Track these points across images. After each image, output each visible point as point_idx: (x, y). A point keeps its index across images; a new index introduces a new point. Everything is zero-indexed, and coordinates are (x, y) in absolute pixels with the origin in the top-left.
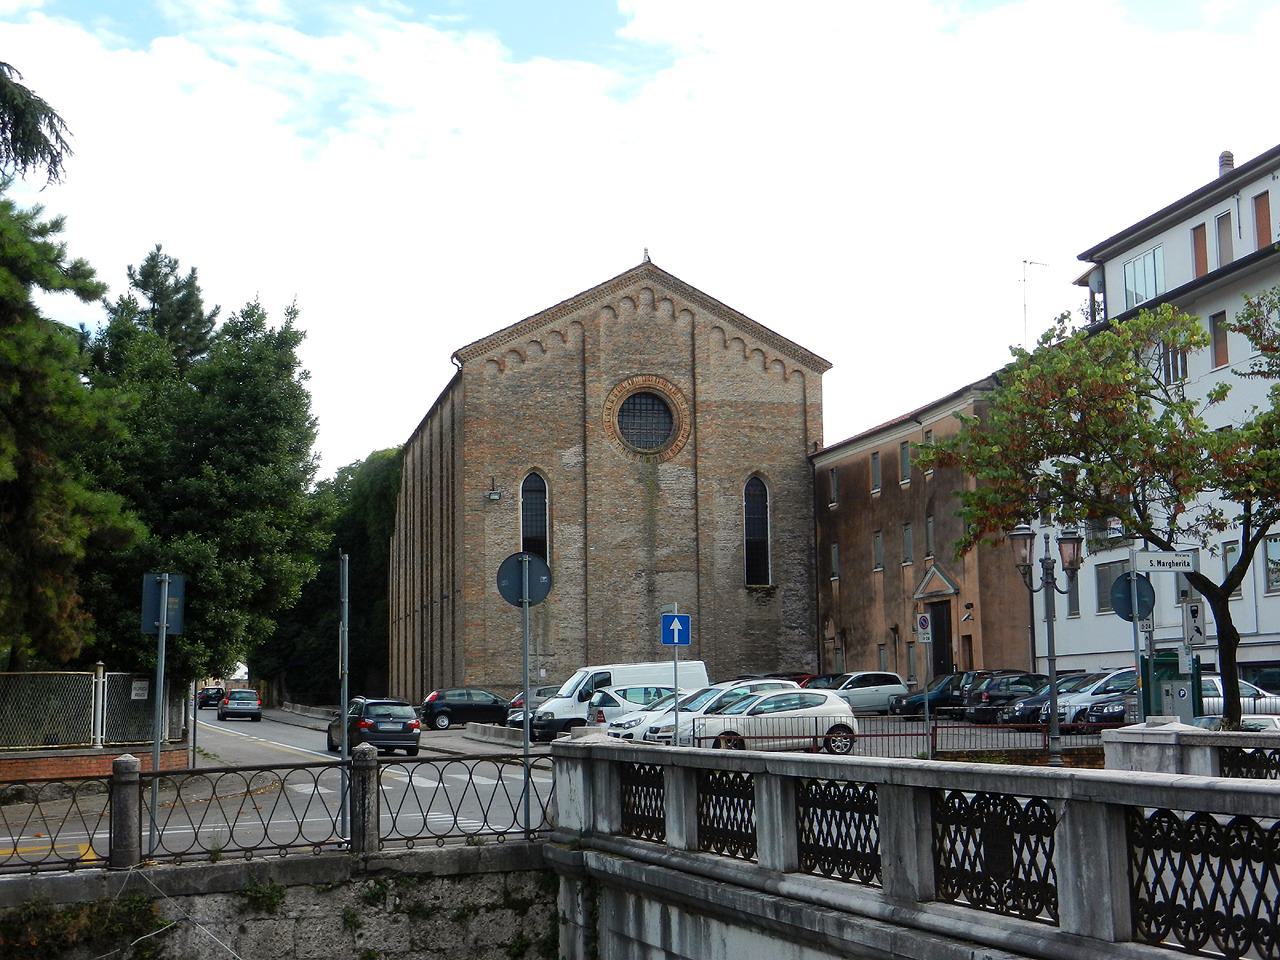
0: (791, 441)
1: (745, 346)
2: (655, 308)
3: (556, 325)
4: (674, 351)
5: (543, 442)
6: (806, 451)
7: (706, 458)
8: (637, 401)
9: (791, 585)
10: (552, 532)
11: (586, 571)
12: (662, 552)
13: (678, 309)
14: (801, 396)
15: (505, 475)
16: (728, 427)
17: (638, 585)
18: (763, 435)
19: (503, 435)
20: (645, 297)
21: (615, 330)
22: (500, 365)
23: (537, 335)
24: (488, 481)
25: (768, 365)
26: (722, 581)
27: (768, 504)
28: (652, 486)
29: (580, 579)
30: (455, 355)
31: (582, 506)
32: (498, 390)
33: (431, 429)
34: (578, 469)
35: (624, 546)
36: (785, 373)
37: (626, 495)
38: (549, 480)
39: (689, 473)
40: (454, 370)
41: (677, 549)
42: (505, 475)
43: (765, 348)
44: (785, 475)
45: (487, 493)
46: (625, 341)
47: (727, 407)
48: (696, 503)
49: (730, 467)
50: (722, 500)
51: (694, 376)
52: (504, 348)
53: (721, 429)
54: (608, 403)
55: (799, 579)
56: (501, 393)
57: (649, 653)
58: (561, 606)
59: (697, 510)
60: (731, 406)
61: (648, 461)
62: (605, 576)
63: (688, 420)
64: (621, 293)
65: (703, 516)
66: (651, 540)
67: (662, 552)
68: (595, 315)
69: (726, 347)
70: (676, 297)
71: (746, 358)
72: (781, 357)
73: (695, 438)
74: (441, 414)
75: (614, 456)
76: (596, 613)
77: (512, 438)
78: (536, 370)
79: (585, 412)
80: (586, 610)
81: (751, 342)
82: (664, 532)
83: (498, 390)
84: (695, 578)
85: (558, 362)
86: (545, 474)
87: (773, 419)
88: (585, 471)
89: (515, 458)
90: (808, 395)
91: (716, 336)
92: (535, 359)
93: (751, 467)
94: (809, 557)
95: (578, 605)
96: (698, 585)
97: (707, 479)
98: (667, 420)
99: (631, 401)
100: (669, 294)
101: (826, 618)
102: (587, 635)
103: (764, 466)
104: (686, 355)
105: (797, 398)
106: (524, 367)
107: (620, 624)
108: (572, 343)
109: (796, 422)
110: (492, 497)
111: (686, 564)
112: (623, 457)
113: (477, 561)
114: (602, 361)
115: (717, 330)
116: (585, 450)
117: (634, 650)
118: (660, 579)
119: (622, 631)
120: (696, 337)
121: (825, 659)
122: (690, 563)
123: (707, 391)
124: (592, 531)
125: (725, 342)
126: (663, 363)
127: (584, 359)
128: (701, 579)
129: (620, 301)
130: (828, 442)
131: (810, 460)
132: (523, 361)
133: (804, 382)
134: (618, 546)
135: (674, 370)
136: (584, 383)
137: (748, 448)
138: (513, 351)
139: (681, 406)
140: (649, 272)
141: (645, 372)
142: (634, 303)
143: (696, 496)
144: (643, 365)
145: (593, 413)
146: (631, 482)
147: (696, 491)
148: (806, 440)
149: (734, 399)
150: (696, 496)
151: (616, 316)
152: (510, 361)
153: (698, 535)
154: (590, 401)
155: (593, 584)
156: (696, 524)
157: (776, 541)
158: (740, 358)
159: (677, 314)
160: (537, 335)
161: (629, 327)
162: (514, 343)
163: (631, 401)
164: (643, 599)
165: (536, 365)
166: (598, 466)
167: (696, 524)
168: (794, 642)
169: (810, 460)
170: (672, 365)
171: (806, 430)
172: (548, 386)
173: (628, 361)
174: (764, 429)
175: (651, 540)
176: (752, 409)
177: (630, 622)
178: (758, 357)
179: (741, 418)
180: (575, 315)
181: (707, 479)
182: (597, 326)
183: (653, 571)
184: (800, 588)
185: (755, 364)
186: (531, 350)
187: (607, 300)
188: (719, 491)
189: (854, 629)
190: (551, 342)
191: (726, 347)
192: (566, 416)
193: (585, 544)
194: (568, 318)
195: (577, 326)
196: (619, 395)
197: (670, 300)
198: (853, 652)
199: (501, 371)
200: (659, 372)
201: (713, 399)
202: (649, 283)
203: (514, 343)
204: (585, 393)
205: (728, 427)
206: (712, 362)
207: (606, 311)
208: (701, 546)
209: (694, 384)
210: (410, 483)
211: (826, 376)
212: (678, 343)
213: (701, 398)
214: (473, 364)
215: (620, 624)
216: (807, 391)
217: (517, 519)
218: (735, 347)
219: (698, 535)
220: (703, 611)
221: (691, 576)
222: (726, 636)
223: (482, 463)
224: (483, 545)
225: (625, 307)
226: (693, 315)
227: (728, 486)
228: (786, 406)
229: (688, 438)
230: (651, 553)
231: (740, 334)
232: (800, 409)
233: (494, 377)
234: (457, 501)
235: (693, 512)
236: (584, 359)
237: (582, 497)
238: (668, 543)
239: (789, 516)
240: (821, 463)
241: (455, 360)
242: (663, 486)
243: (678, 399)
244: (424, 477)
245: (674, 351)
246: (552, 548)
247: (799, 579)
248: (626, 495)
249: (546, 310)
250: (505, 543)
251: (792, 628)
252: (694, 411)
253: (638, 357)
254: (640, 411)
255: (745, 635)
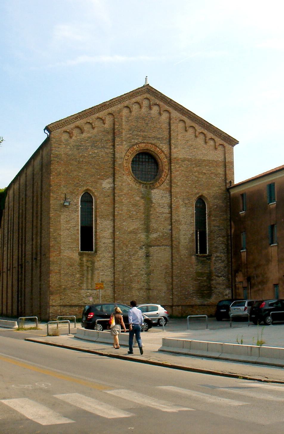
0: (219, 180)
1: (196, 130)
2: (150, 108)
3: (100, 115)
4: (160, 131)
5: (92, 176)
6: (226, 185)
7: (176, 187)
8: (141, 156)
9: (218, 254)
10: (96, 224)
11: (114, 245)
12: (154, 236)
13: (162, 109)
14: (223, 157)
15: (72, 193)
16: (187, 172)
17: (141, 253)
18: (205, 177)
19: (72, 171)
20: (145, 103)
21: (130, 119)
22: (70, 134)
23: (90, 120)
24: (63, 196)
25: (207, 141)
26: (184, 252)
27: (206, 212)
28: (148, 199)
29: (111, 249)
30: (47, 128)
31: (112, 210)
32: (69, 147)
33: (26, 174)
34: (110, 191)
35: (134, 232)
36: (215, 146)
37: (134, 205)
38: (95, 196)
39: (168, 195)
40: (45, 137)
41: (161, 234)
42: (72, 193)
43: (205, 132)
44: (215, 198)
45: (62, 202)
46: (135, 124)
47: (186, 162)
48: (171, 211)
49: (188, 192)
50: (184, 209)
51: (170, 145)
52: (72, 126)
53: (183, 172)
54: (126, 157)
55: (222, 251)
56: (71, 149)
57: (147, 289)
58: (101, 263)
59: (171, 214)
60: (189, 161)
61: (146, 187)
62: (124, 248)
63: (167, 168)
64: (134, 100)
65: (174, 218)
66: (148, 230)
67: (154, 236)
68: (120, 111)
69: (186, 131)
70: (161, 104)
71: (196, 137)
72: (214, 137)
73: (171, 177)
74: (33, 164)
75: (129, 184)
76: (119, 268)
77: (75, 173)
78: (90, 138)
79: (114, 162)
80: (114, 266)
81: (199, 129)
82: (154, 225)
83: (69, 147)
84: (170, 250)
85: (100, 134)
86: (93, 193)
87: (210, 169)
88: (114, 192)
89: (77, 183)
90: (227, 157)
91: (181, 125)
92: (89, 132)
93: (198, 193)
94: (227, 240)
95: (109, 263)
96: (172, 253)
97: (177, 198)
98: (156, 167)
99: (137, 156)
100: (158, 102)
101: (237, 271)
102: (114, 279)
103: (205, 193)
104: (166, 134)
105: (221, 159)
106: (83, 135)
107: (131, 274)
108: (108, 125)
109: (221, 171)
110: (65, 204)
111: (165, 242)
112: (134, 185)
113: (56, 238)
114: (124, 134)
115: (182, 122)
116: (114, 181)
117: (139, 287)
118: (152, 250)
119: (132, 277)
120: (171, 125)
121: (236, 293)
122: (168, 242)
123: (178, 153)
124: (118, 224)
125: (186, 128)
126: (154, 137)
127: (114, 133)
128: (173, 251)
129: (133, 104)
130: (237, 181)
131: (228, 190)
132: (82, 133)
133: (225, 150)
134: (130, 232)
135: (160, 141)
136: (114, 146)
137: (197, 183)
138: (77, 127)
139: (163, 160)
140: (148, 90)
141: (145, 141)
142: (140, 105)
143: (171, 207)
144: (144, 137)
145: (119, 162)
146: (138, 198)
147: (171, 204)
148: (226, 179)
149: (190, 157)
150: (171, 207)
151: (131, 112)
152: (76, 132)
153: (172, 227)
154: (117, 155)
155: (118, 252)
156: (171, 221)
157: (211, 232)
158: (193, 136)
159: (162, 112)
160: (90, 120)
161: (137, 118)
162: (78, 123)
163: (137, 156)
164: (143, 260)
165: (89, 135)
166: (121, 190)
167: (171, 221)
168: (220, 284)
169: (228, 190)
170: (159, 138)
171: (225, 175)
172: (95, 147)
173: (137, 135)
174: (205, 173)
175: (148, 230)
176: (199, 163)
177: (137, 272)
178: (202, 136)
179: (194, 168)
180: (110, 110)
181: (177, 198)
182: (121, 116)
183: (148, 246)
184: (223, 256)
185: (200, 140)
186: (87, 127)
187: (126, 103)
188: (182, 205)
189: (257, 277)
190: (97, 123)
191: (186, 131)
192: (104, 162)
193: (114, 231)
194: (106, 112)
195: (110, 116)
196: (132, 152)
197: (158, 105)
198: (255, 288)
199: (71, 137)
200: (153, 142)
201: (180, 157)
202: (148, 96)
203: (78, 123)
204: (114, 151)
205: (187, 172)
206: (179, 138)
207: (126, 109)
208: (174, 233)
209: (170, 149)
210: (11, 204)
211: (236, 148)
212: (162, 127)
213: (174, 156)
214: (56, 133)
215: (131, 274)
216: (226, 155)
217: (78, 216)
218: (191, 131)
219: (172, 227)
220: (174, 267)
221: (168, 248)
222: (185, 280)
223: (60, 186)
224: (60, 229)
225: (135, 107)
226: (170, 113)
227: (187, 202)
228: (216, 162)
229: (167, 176)
230: (147, 237)
231: (193, 124)
232: (222, 164)
233: (67, 141)
234: (44, 207)
235: (169, 215)
236: (114, 133)
237: (112, 206)
238: (156, 231)
239: (217, 218)
240: (233, 192)
241: (46, 131)
242: (154, 201)
243: (162, 156)
244: (21, 199)
245: (160, 131)
246: (96, 232)
247: (222, 251)
248: (134, 205)
249: (95, 107)
250: (71, 229)
251: (218, 276)
252: (170, 162)
253: (142, 133)
254: (142, 162)
255: (196, 280)
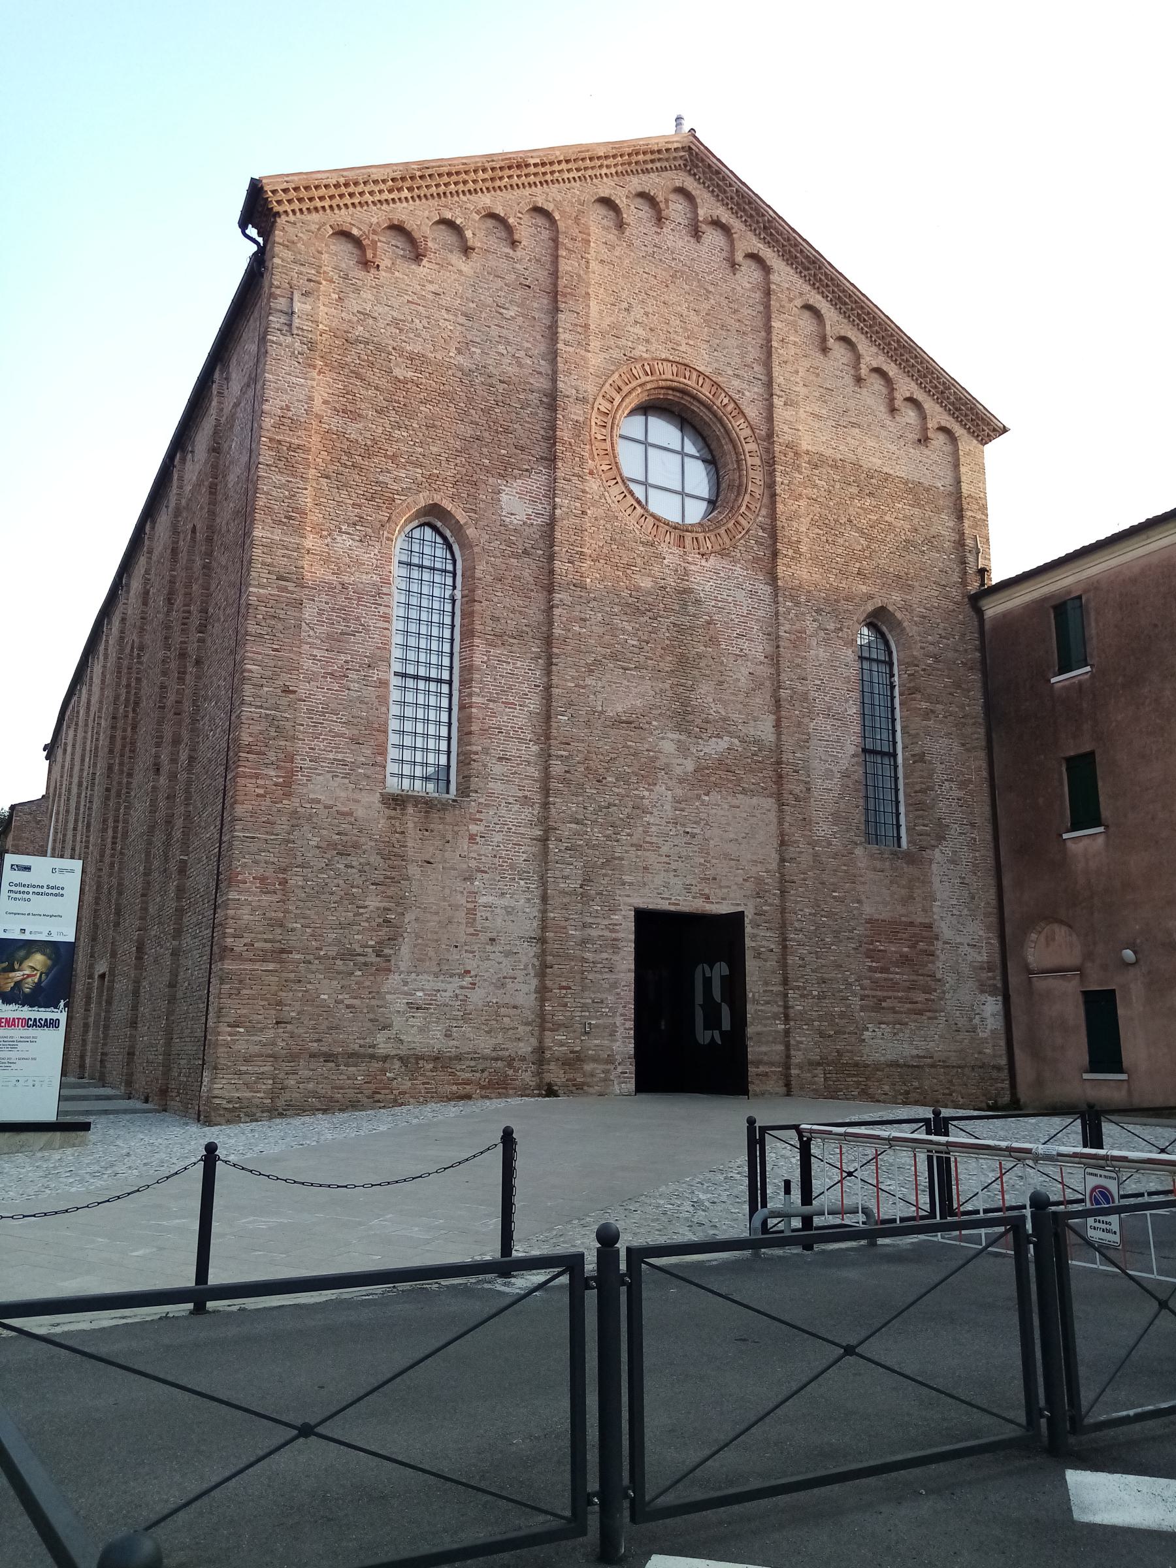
0: (940, 560)
1: (858, 358)
6: (964, 583)
14: (949, 480)
54: (600, 399)
75: (611, 517)
91: (807, 323)
102: (544, 928)
103: (894, 599)
105: (942, 482)
124: (566, 678)
131: (975, 600)
134: (618, 722)
155: (563, 806)
178: (876, 383)
197: (725, 229)
211: (993, 451)
213: (784, 433)
218: (839, 352)
226: (766, 269)
228: (927, 490)
239: (940, 707)
240: (994, 608)
